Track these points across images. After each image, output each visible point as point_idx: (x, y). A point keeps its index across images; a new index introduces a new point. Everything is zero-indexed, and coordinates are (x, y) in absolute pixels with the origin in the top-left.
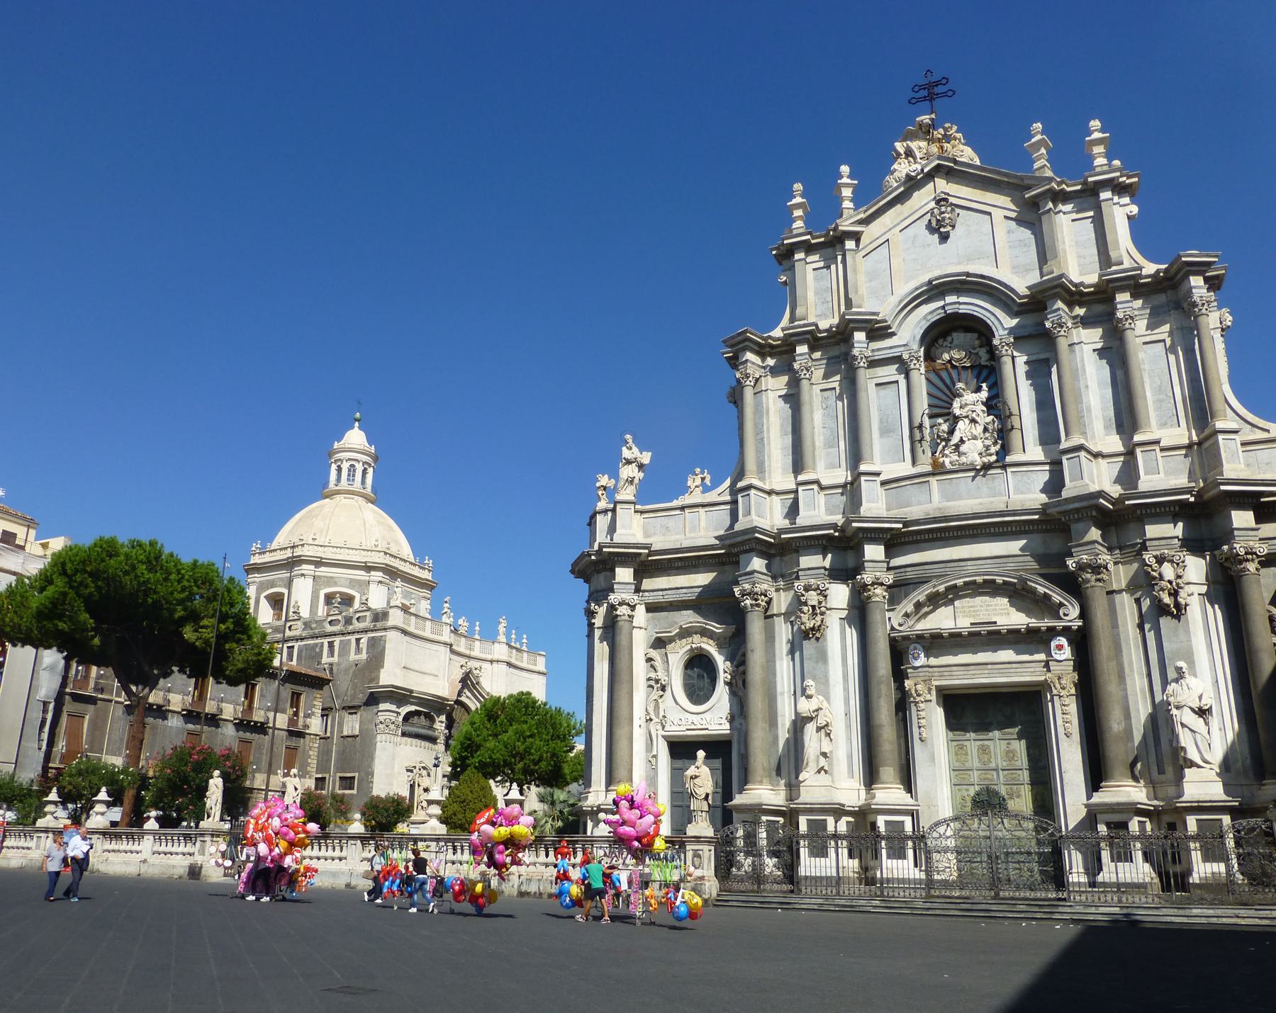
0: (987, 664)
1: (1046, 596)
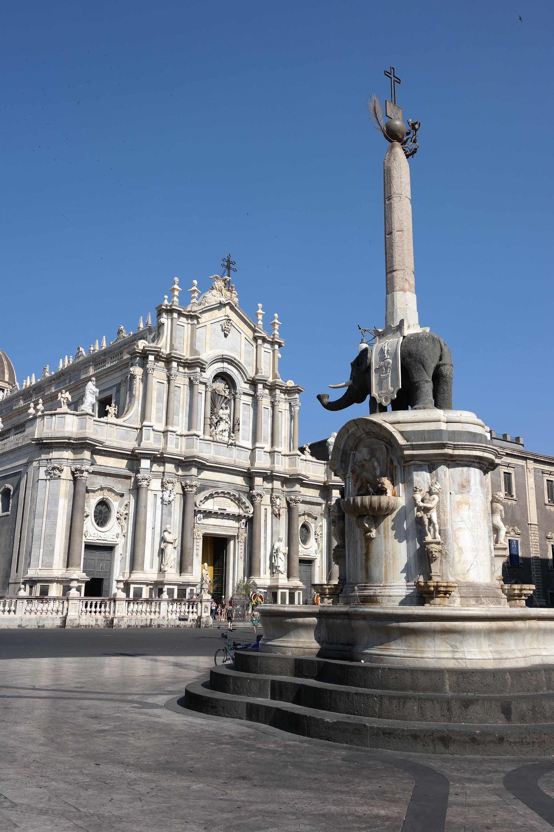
0: (221, 526)
1: (244, 503)
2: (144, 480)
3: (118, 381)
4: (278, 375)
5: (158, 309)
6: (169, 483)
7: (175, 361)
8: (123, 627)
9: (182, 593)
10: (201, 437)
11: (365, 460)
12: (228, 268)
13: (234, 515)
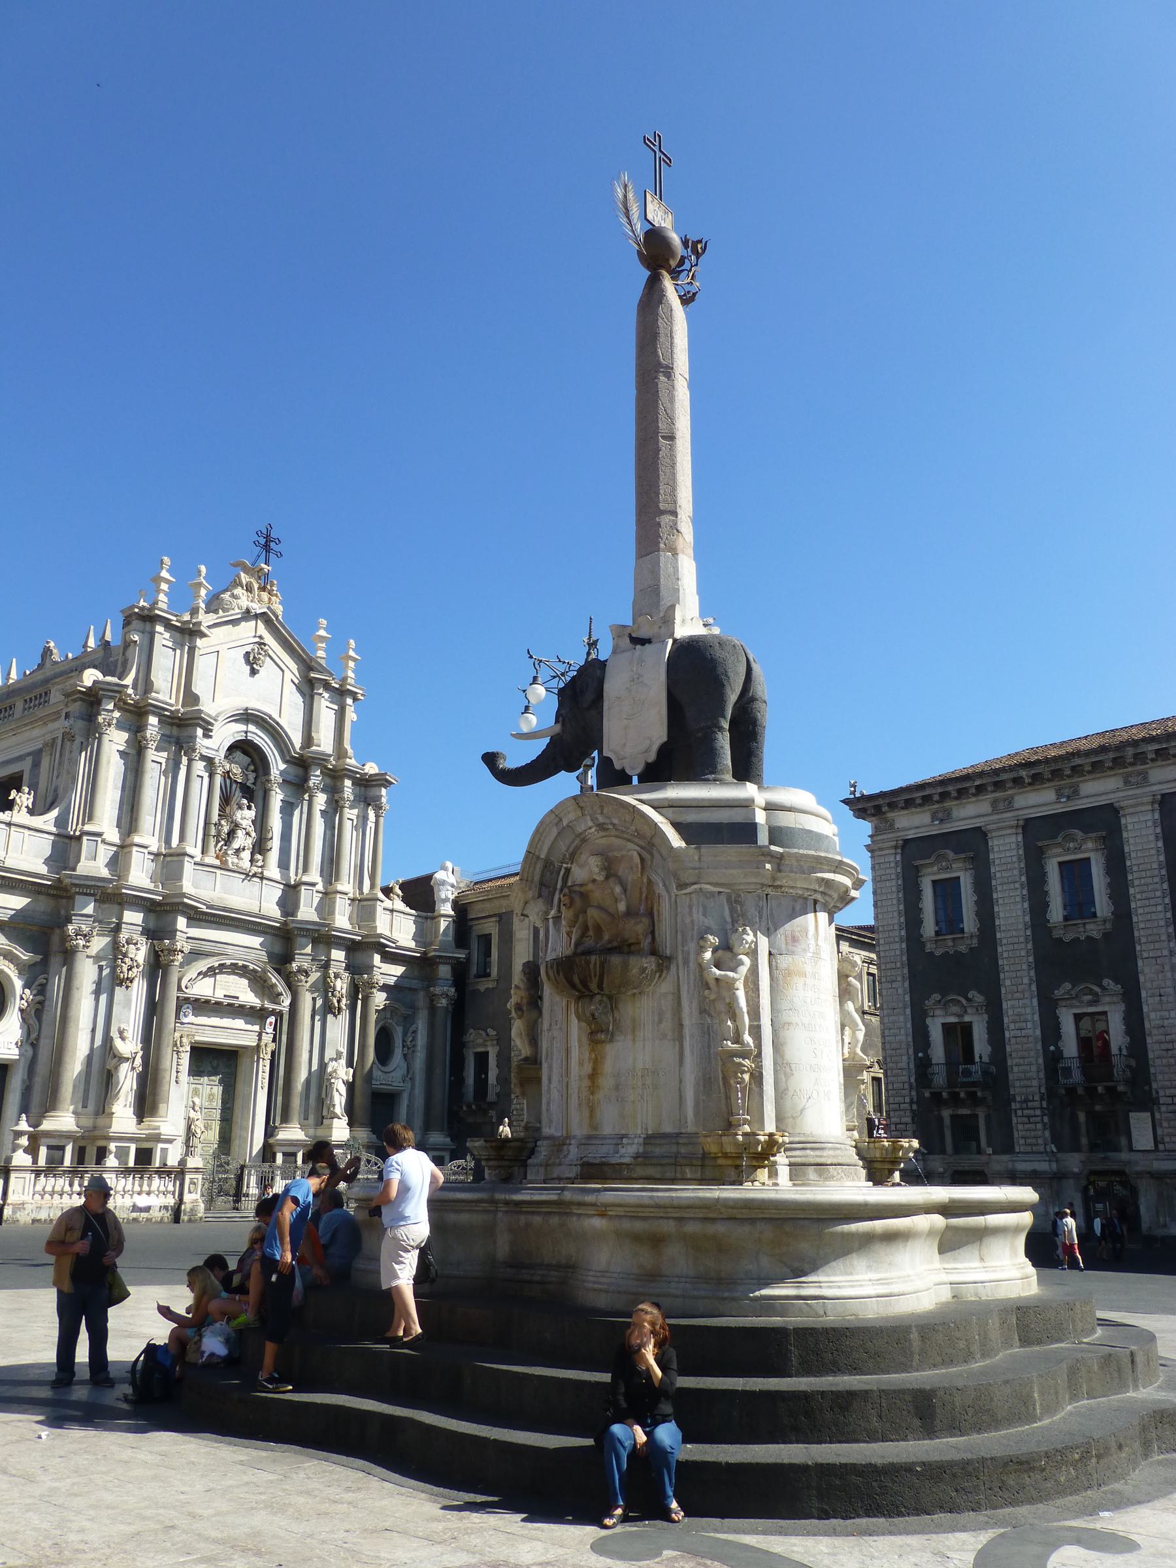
1: (273, 986)
2: (78, 937)
3: (38, 745)
4: (350, 752)
5: (126, 615)
6: (128, 943)
7: (154, 714)
8: (22, 1222)
9: (144, 1156)
10: (198, 859)
11: (594, 881)
12: (267, 547)
13: (252, 1008)
